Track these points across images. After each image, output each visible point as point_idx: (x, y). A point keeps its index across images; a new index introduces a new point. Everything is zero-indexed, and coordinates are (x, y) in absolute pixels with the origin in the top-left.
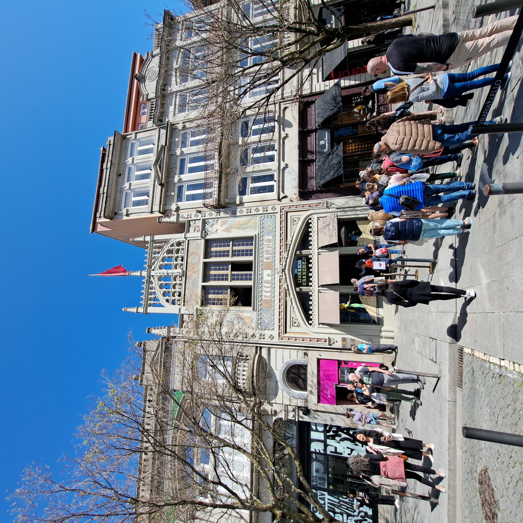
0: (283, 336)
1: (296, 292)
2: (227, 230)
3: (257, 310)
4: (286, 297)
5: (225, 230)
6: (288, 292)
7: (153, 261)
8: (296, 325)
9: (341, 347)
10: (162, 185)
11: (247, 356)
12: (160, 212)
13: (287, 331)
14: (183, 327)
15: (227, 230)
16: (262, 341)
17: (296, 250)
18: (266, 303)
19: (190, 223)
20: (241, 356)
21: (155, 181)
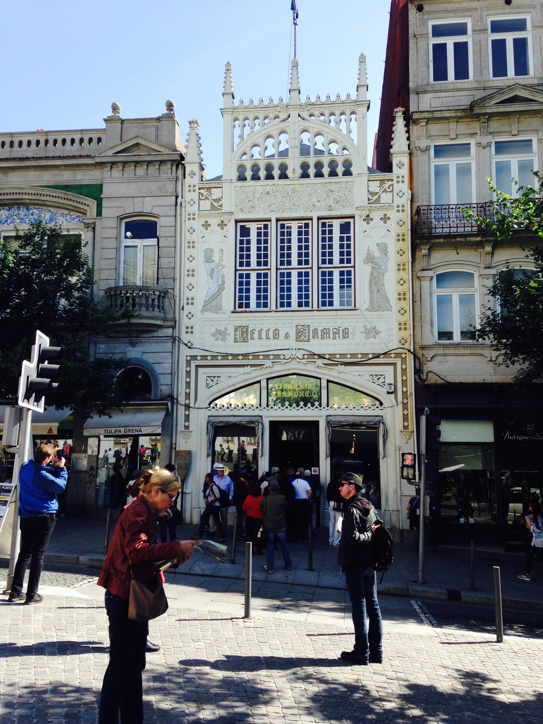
0: (192, 362)
1: (259, 382)
2: (370, 259)
3: (230, 319)
4: (252, 366)
5: (368, 253)
6: (259, 368)
7: (317, 113)
8: (209, 381)
9: (177, 449)
10: (472, 106)
11: (159, 307)
12: (412, 113)
13: (199, 369)
14: (200, 191)
15: (370, 259)
16: (184, 330)
17: (328, 381)
18: (242, 333)
19: (388, 180)
20: (159, 296)
21: (484, 89)
